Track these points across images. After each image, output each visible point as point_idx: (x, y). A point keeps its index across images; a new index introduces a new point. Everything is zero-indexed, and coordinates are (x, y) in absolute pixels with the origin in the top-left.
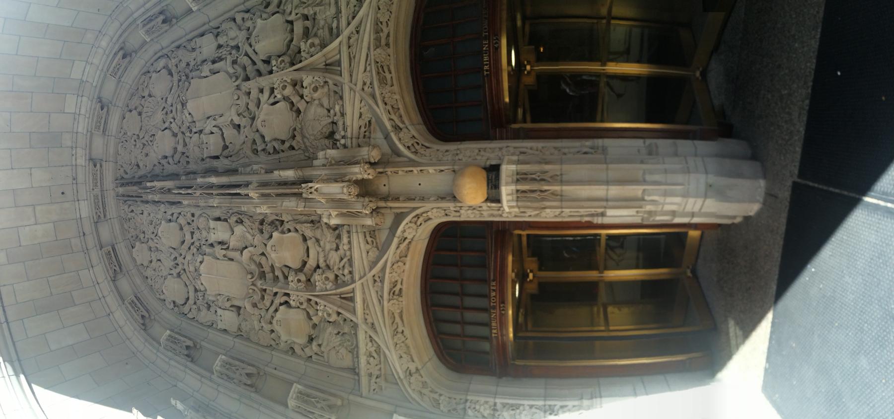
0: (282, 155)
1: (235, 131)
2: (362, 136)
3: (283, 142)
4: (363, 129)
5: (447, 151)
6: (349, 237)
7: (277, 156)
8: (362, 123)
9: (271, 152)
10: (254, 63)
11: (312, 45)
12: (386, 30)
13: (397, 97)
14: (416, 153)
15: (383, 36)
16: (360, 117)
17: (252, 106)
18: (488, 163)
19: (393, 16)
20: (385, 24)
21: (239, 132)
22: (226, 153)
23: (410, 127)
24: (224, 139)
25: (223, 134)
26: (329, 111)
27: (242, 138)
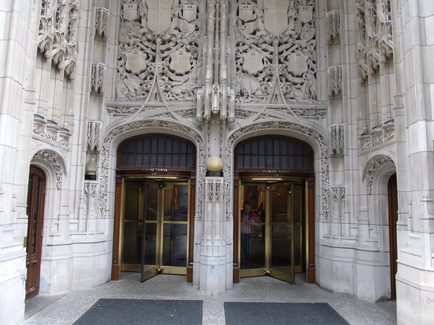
0: (235, 62)
1: (252, 31)
2: (240, 112)
3: (241, 65)
4: (243, 113)
5: (230, 152)
6: (189, 101)
7: (234, 59)
8: (246, 113)
9: (238, 57)
10: (287, 50)
11: (287, 88)
12: (286, 127)
13: (256, 130)
14: (230, 138)
15: (284, 126)
16: (249, 112)
17: (264, 46)
18: (224, 171)
19: (292, 130)
20: (289, 127)
21: (251, 34)
22: (240, 22)
23: (242, 135)
24: (248, 22)
25: (251, 21)
26: (254, 94)
27: (247, 36)
